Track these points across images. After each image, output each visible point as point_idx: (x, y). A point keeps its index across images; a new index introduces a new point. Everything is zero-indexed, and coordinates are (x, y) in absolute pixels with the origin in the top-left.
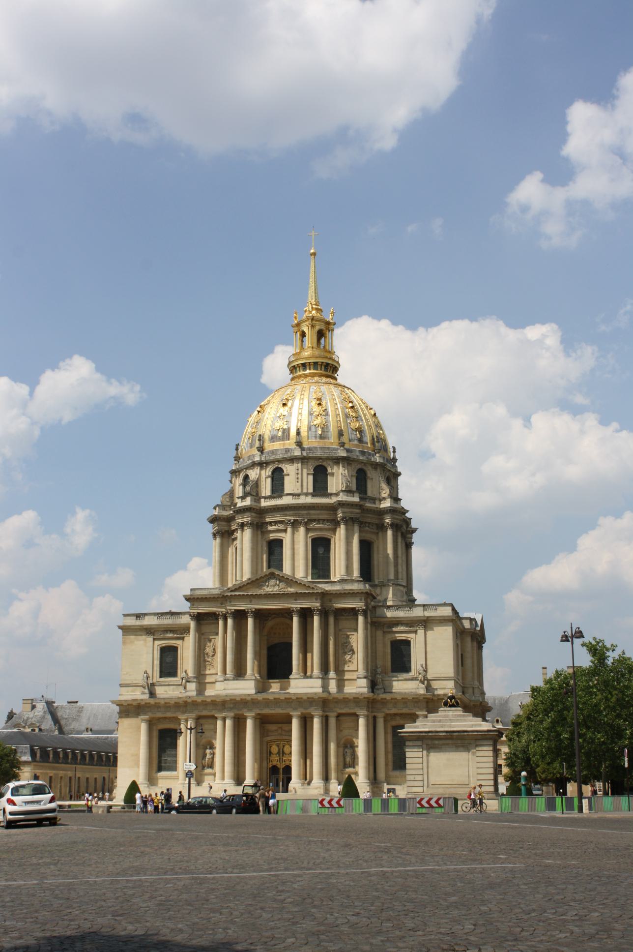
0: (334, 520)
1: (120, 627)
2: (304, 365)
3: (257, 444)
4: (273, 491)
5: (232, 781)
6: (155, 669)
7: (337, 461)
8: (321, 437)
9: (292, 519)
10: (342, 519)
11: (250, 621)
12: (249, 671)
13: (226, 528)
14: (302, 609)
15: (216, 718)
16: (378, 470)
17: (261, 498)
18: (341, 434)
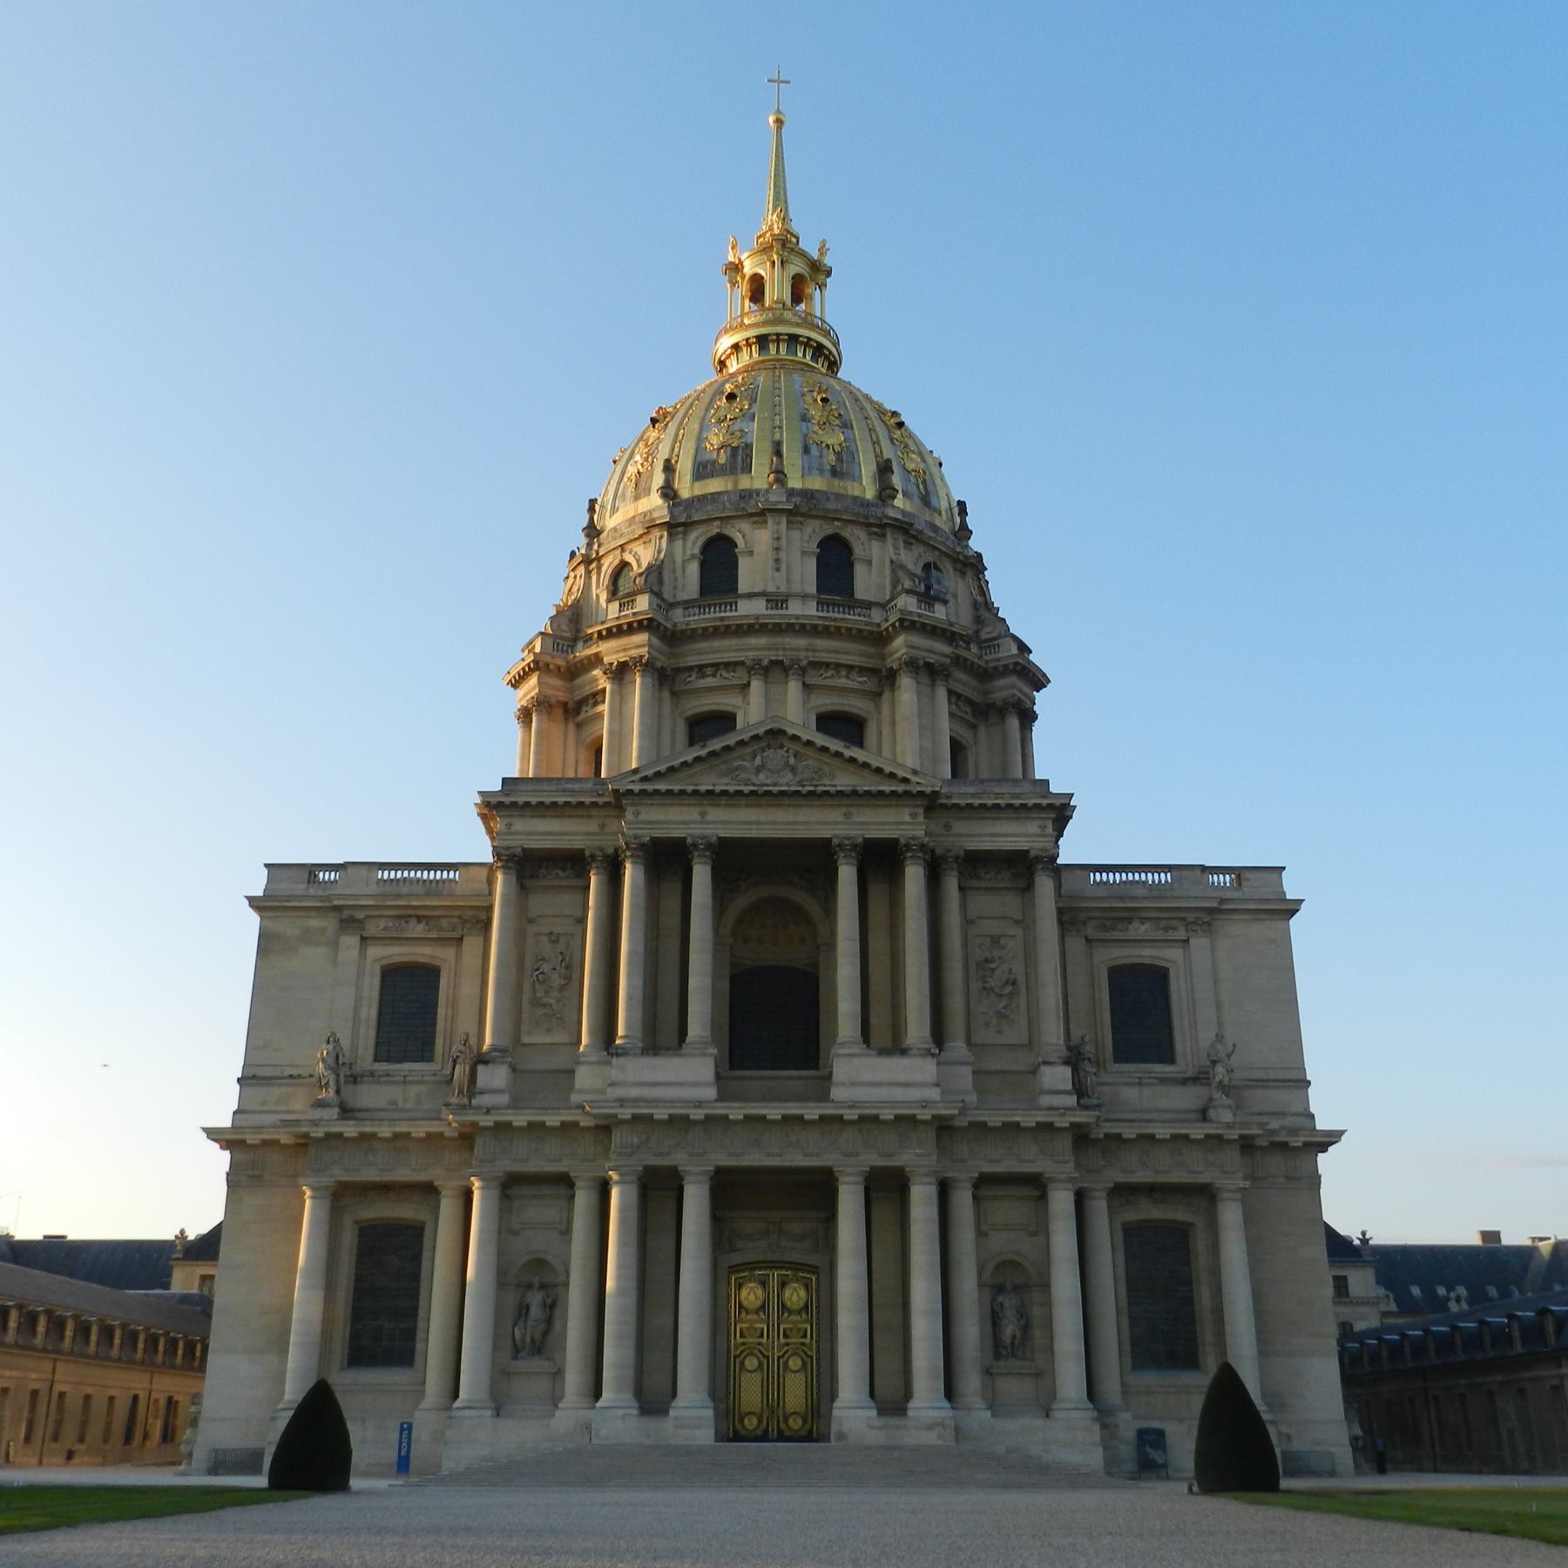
0: (873, 671)
1: (253, 902)
2: (762, 341)
3: (659, 479)
4: (701, 594)
5: (628, 1398)
6: (362, 1031)
7: (881, 527)
8: (835, 472)
9: (767, 656)
10: (912, 665)
11: (701, 875)
12: (698, 1026)
13: (562, 696)
14: (868, 843)
15: (565, 1182)
16: (969, 573)
17: (672, 606)
18: (884, 469)
